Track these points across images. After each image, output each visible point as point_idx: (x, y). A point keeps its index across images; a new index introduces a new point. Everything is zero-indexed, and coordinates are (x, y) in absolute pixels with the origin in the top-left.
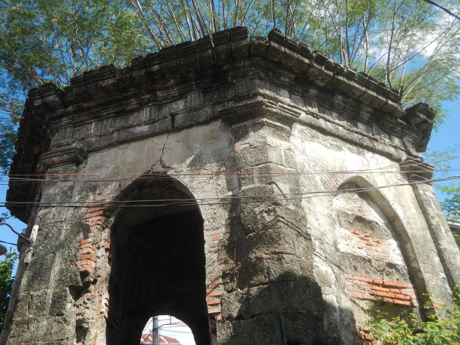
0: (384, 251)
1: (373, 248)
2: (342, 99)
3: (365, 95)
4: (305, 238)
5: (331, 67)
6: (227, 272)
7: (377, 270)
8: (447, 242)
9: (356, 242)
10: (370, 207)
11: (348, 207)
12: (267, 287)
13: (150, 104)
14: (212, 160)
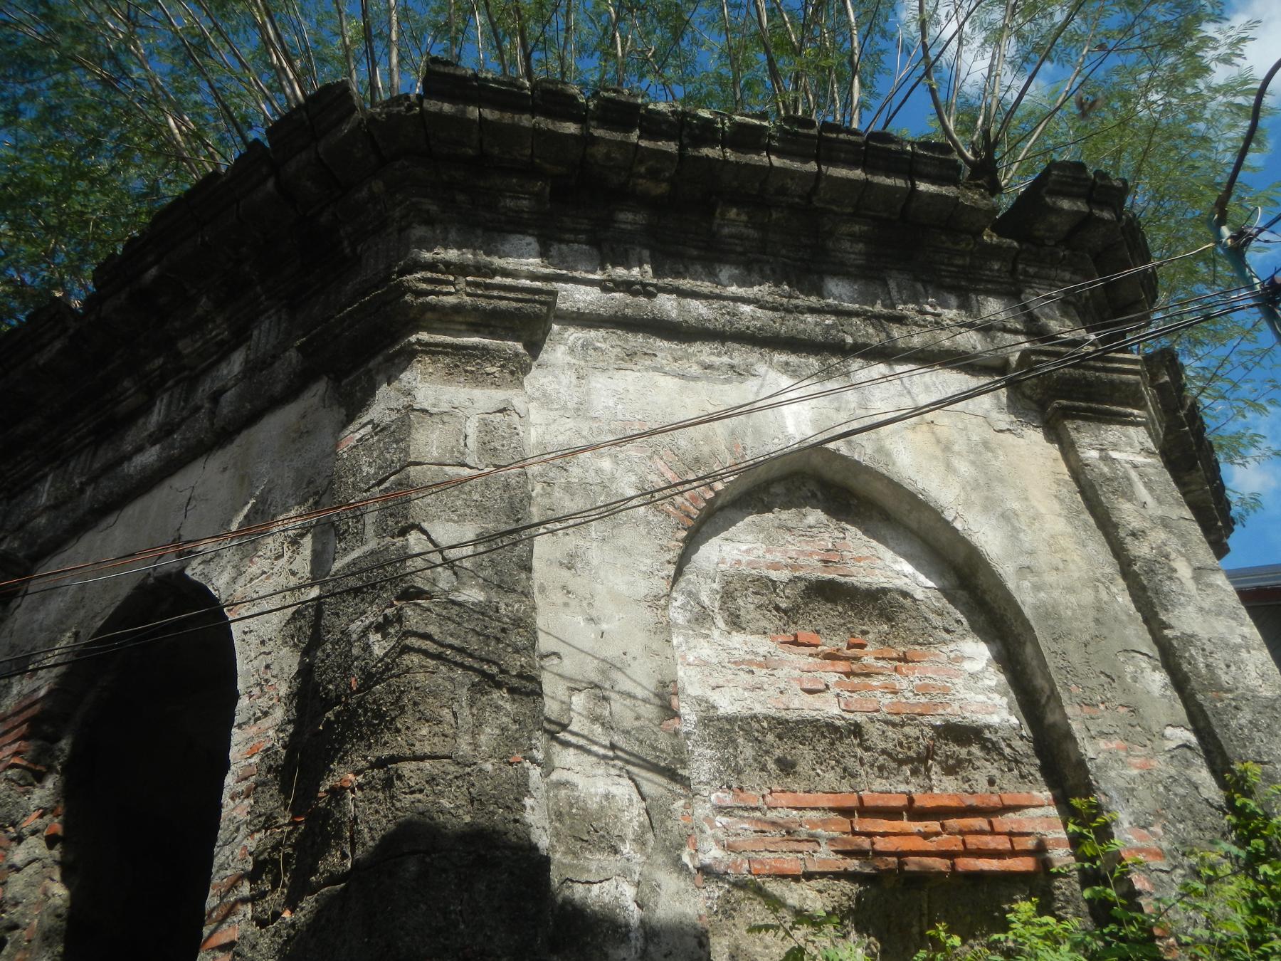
0: (927, 686)
1: (874, 682)
2: (744, 218)
3: (822, 185)
4: (512, 691)
5: (664, 127)
6: (261, 858)
7: (895, 760)
8: (1201, 609)
9: (796, 673)
10: (874, 543)
11: (778, 557)
12: (342, 889)
13: (170, 383)
14: (291, 501)
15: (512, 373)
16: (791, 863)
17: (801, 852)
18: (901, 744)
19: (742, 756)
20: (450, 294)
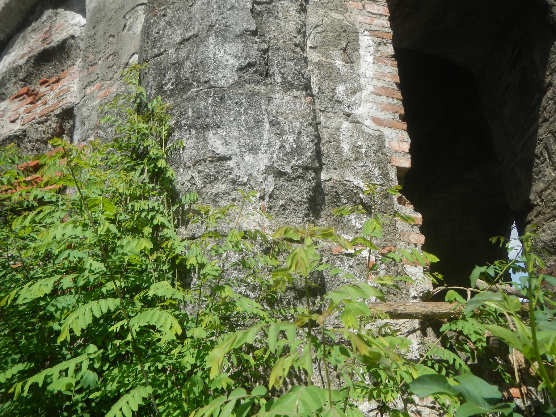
18: (44, 132)
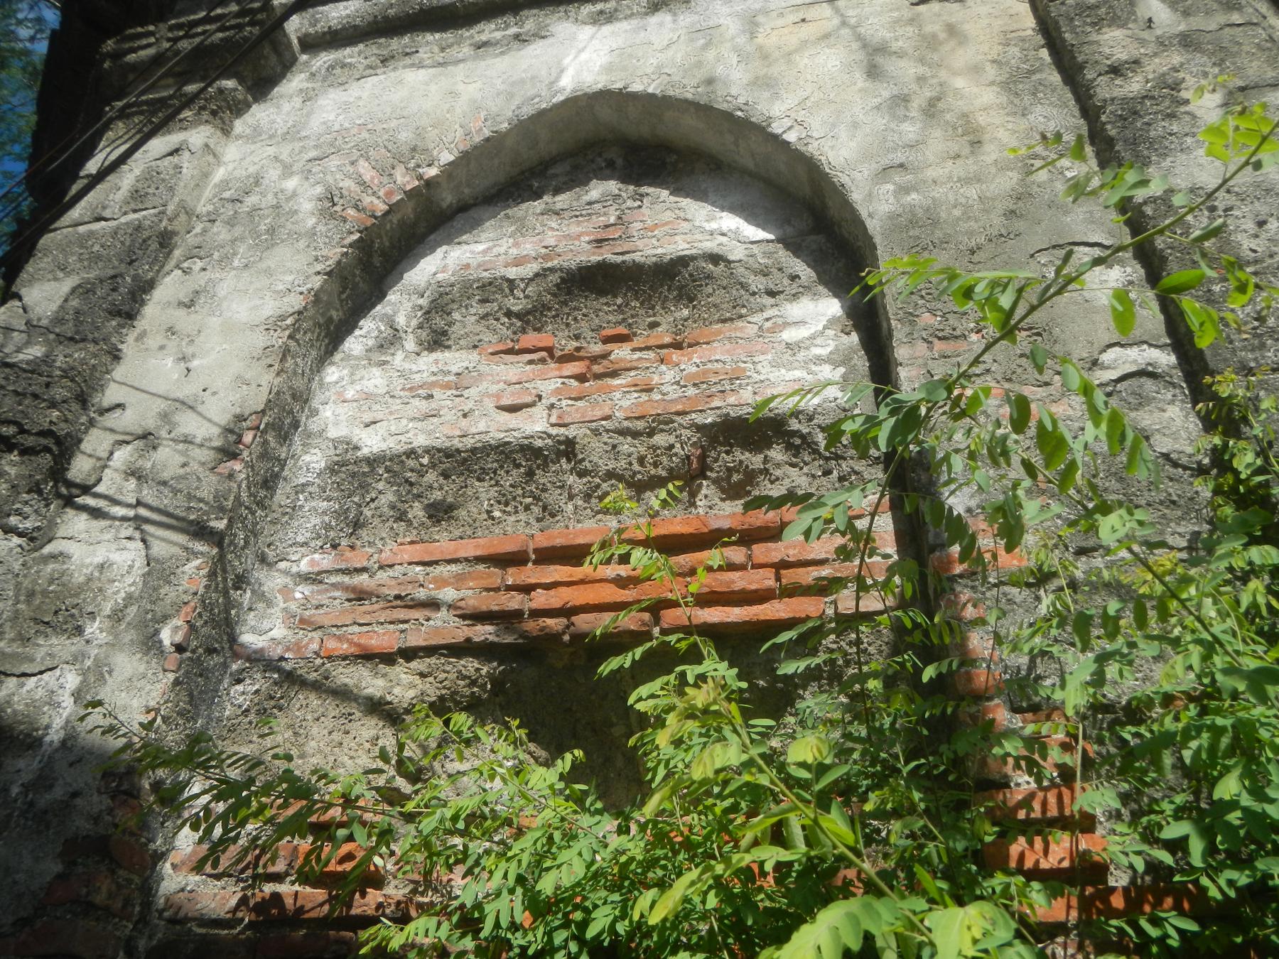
1: (617, 382)
4: (25, 452)
10: (686, 202)
11: (529, 247)
15: (214, 113)
16: (384, 638)
17: (406, 622)
18: (641, 460)
19: (372, 505)
20: (149, 45)
